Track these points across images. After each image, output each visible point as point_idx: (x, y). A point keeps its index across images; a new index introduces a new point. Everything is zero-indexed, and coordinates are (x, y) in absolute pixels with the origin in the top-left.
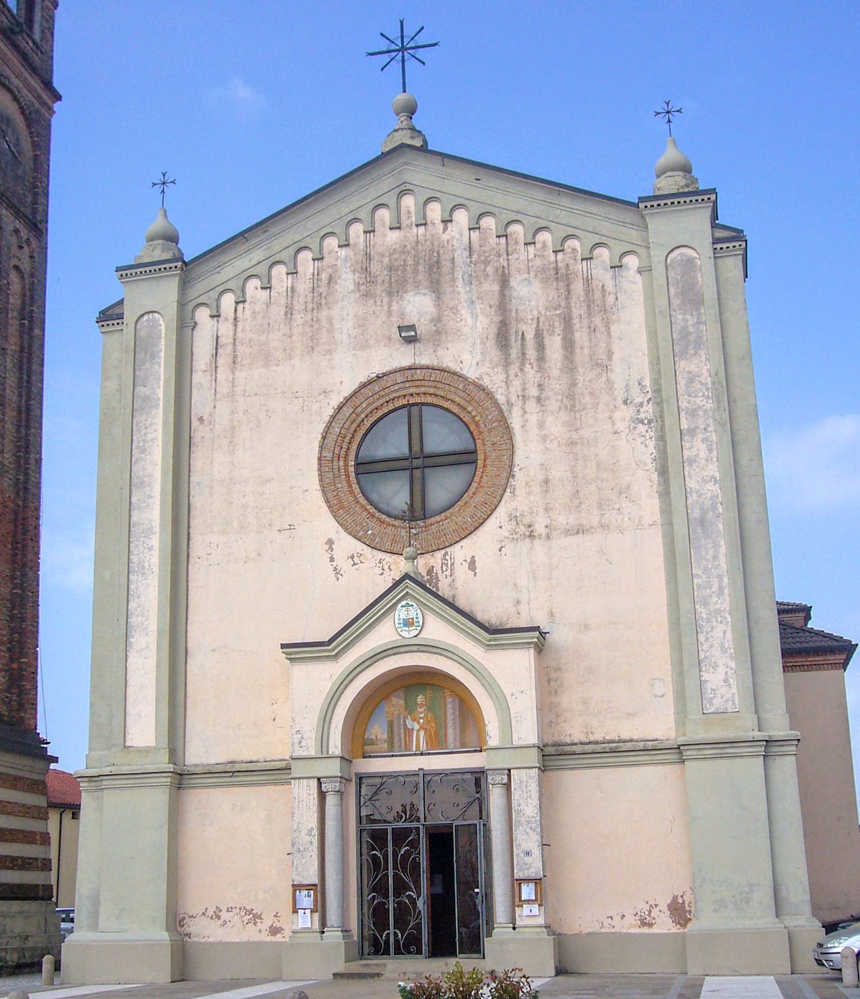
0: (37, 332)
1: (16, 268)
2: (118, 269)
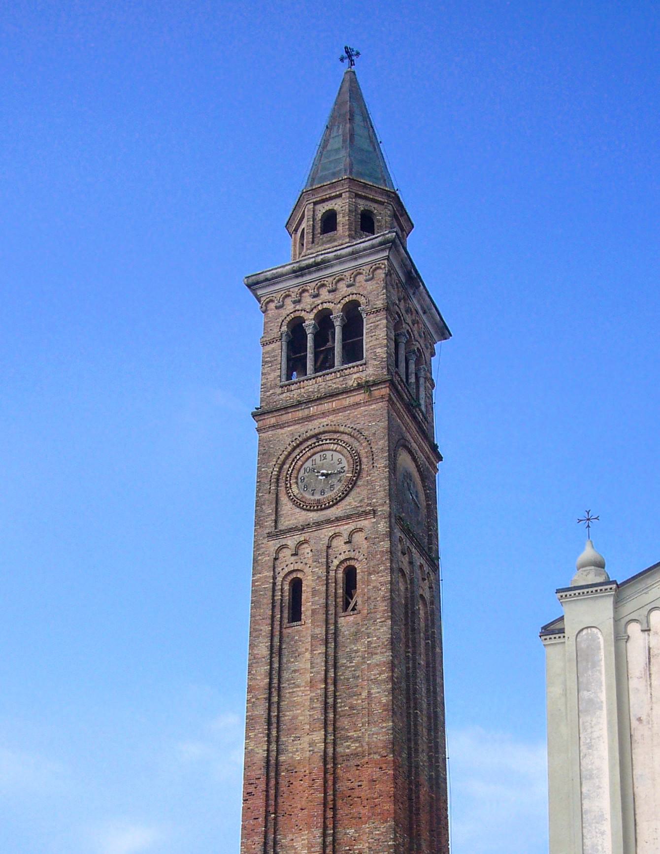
0: (438, 650)
1: (421, 595)
2: (558, 591)
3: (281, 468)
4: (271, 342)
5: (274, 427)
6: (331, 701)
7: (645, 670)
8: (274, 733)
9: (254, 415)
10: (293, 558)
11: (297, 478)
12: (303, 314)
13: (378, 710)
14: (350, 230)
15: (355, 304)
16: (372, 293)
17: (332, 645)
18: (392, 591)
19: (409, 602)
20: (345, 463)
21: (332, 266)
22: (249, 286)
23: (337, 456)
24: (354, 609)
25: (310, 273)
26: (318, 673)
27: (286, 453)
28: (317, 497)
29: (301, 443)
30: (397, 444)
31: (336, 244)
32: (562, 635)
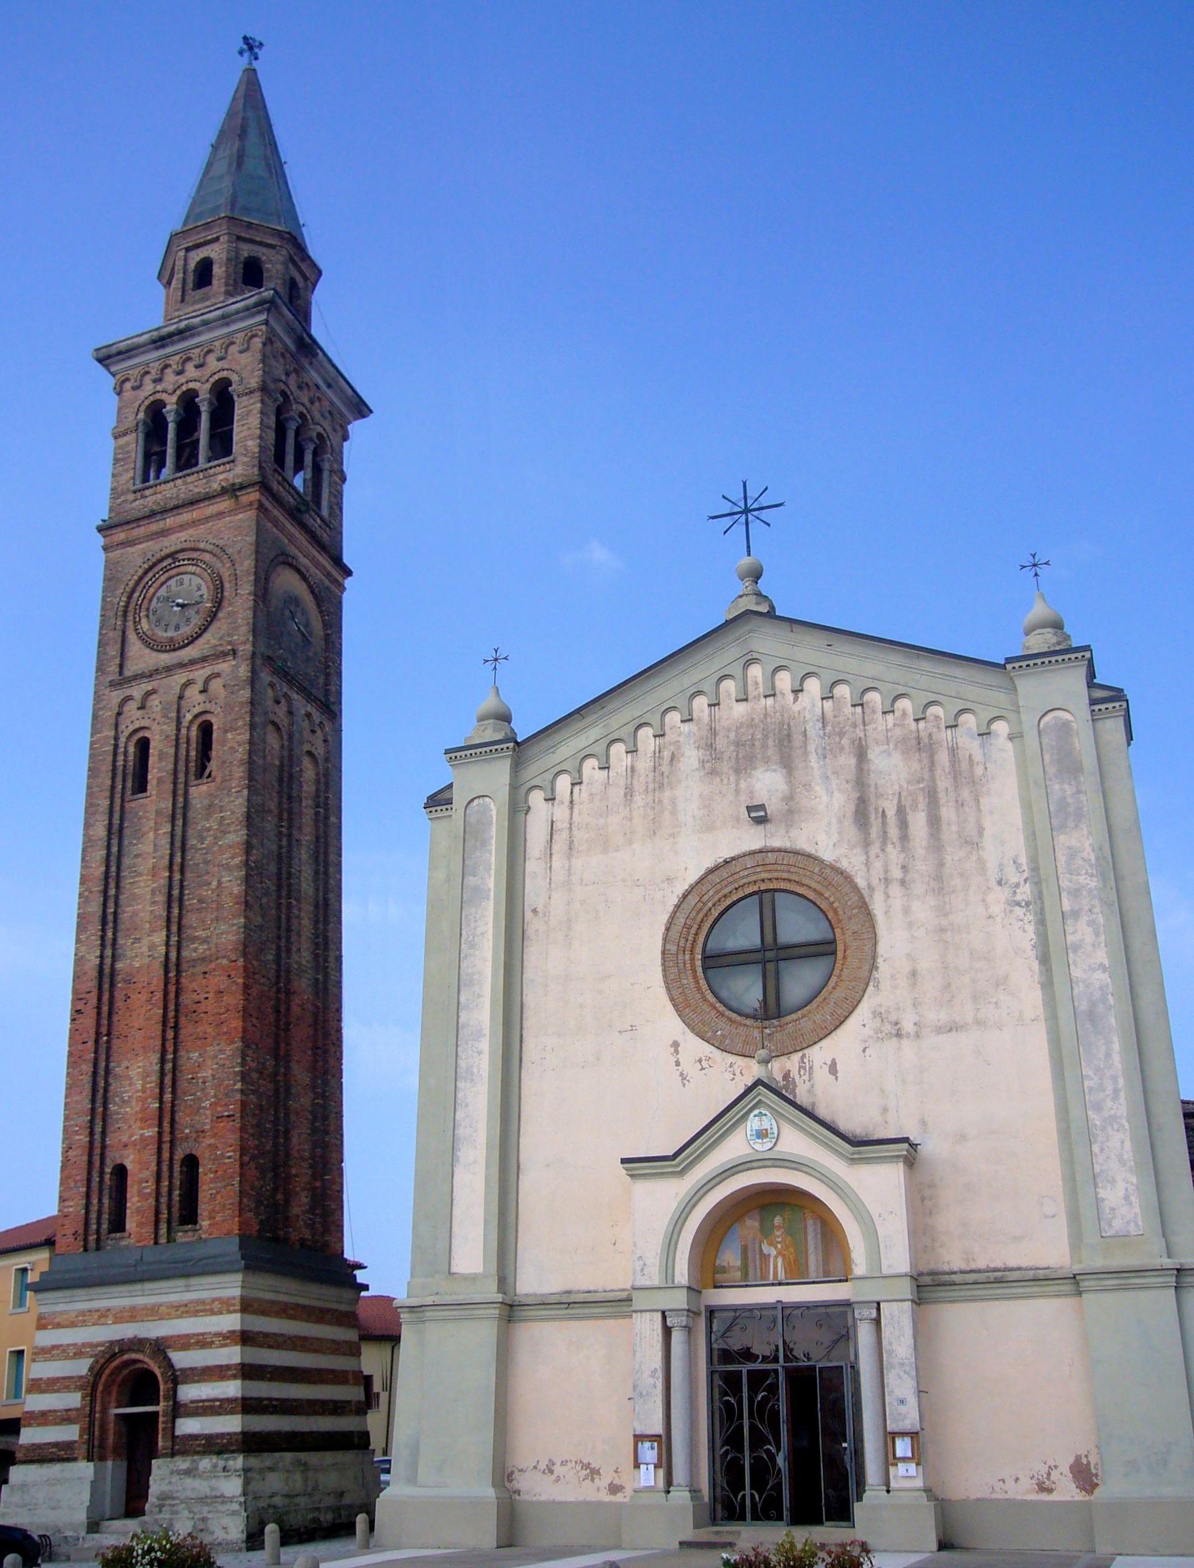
0: (333, 819)
1: (309, 753)
3: (130, 597)
4: (125, 434)
5: (123, 544)
6: (176, 892)
7: (546, 848)
8: (110, 934)
9: (100, 530)
10: (140, 712)
11: (148, 609)
12: (164, 396)
13: (228, 902)
14: (227, 284)
15: (226, 382)
16: (245, 369)
17: (180, 823)
18: (250, 753)
19: (286, 762)
20: (204, 591)
21: (199, 334)
22: (100, 361)
23: (197, 580)
24: (209, 776)
25: (173, 343)
26: (162, 858)
27: (136, 578)
28: (170, 634)
29: (155, 565)
30: (271, 560)
31: (208, 303)
32: (448, 807)
